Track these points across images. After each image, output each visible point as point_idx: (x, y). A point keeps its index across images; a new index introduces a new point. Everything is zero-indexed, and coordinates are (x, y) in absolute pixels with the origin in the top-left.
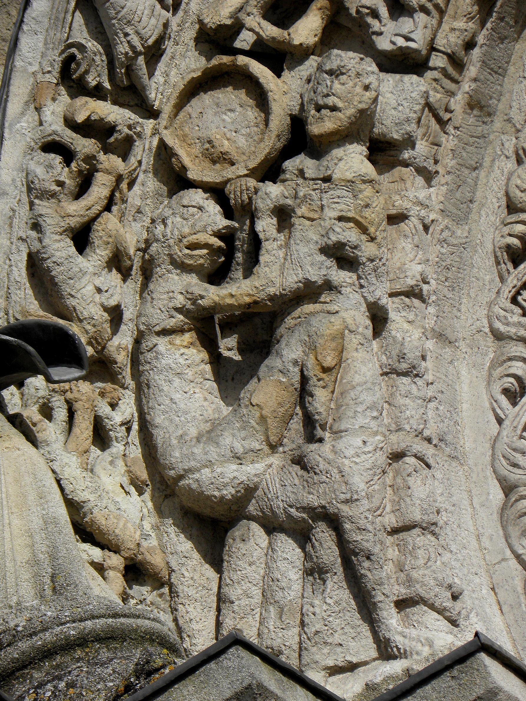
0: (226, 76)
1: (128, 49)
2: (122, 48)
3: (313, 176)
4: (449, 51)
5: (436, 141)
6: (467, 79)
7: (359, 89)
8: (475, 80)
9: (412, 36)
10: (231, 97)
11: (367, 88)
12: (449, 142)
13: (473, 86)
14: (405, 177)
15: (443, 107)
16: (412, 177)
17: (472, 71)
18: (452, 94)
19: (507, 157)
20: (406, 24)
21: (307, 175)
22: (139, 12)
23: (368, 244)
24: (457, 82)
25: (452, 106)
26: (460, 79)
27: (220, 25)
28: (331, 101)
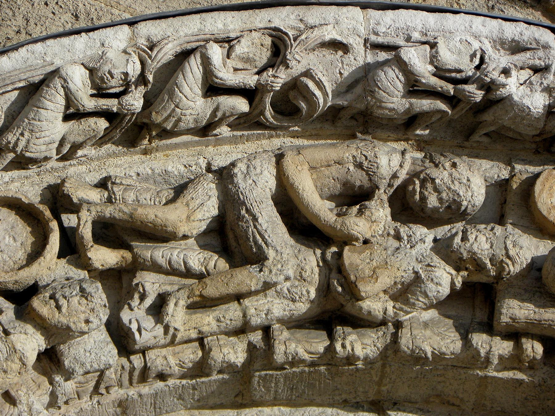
0: (36, 221)
1: (13, 142)
2: (11, 137)
4: (149, 365)
5: (81, 394)
6: (137, 389)
7: (83, 317)
8: (140, 396)
9: (143, 332)
10: (24, 234)
11: (87, 322)
12: (86, 403)
13: (136, 397)
14: (42, 387)
15: (107, 385)
16: (45, 392)
17: (145, 389)
18: (121, 386)
20: (149, 322)
22: (43, 134)
24: (131, 383)
25: (113, 390)
26: (134, 384)
28: (63, 302)
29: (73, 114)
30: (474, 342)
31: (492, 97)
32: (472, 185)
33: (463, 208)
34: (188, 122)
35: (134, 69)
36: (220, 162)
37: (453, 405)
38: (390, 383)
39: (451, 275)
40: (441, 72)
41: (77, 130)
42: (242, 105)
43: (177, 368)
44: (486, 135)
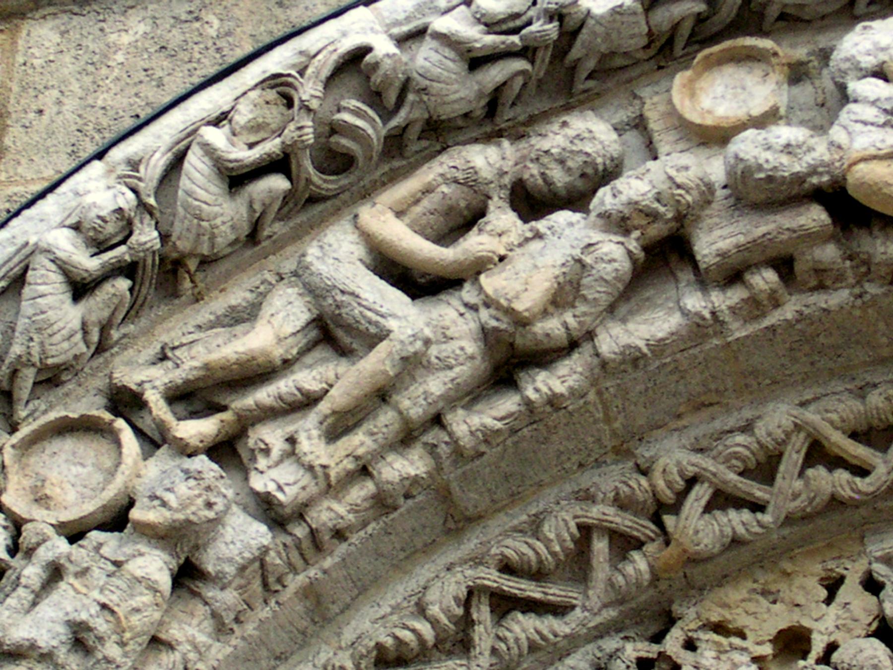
3: (106, 555)
4: (314, 526)
5: (251, 601)
6: (317, 566)
7: (200, 501)
8: (325, 572)
9: (286, 489)
11: (209, 505)
13: (320, 575)
14: (197, 613)
15: (277, 575)
18: (294, 570)
19: (314, 666)
21: (102, 551)
22: (55, 327)
23: (115, 645)
27: (124, 386)
29: (81, 288)
30: (689, 307)
31: (570, 24)
32: (597, 135)
33: (601, 168)
34: (225, 235)
35: (127, 200)
36: (289, 266)
37: (711, 404)
38: (619, 412)
39: (622, 244)
40: (492, 25)
41: (97, 306)
42: (278, 183)
43: (351, 516)
44: (590, 77)
